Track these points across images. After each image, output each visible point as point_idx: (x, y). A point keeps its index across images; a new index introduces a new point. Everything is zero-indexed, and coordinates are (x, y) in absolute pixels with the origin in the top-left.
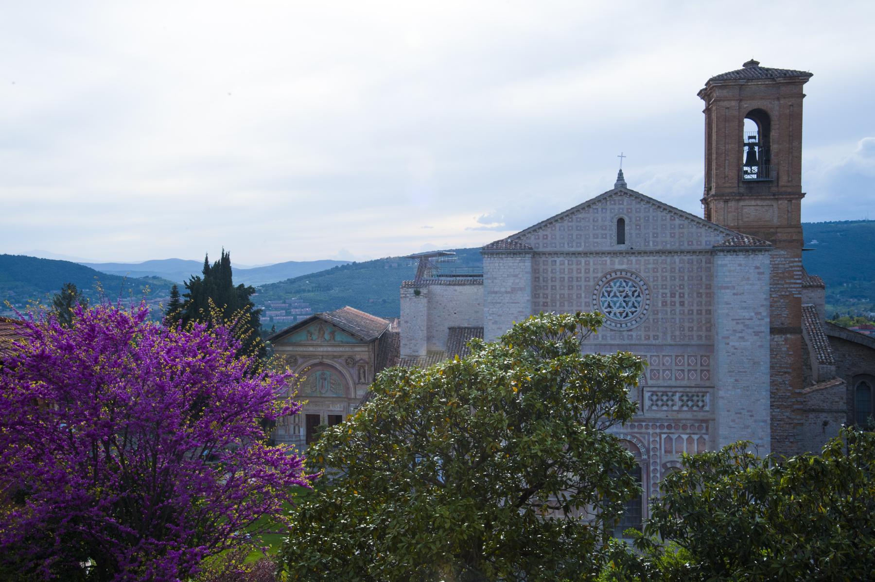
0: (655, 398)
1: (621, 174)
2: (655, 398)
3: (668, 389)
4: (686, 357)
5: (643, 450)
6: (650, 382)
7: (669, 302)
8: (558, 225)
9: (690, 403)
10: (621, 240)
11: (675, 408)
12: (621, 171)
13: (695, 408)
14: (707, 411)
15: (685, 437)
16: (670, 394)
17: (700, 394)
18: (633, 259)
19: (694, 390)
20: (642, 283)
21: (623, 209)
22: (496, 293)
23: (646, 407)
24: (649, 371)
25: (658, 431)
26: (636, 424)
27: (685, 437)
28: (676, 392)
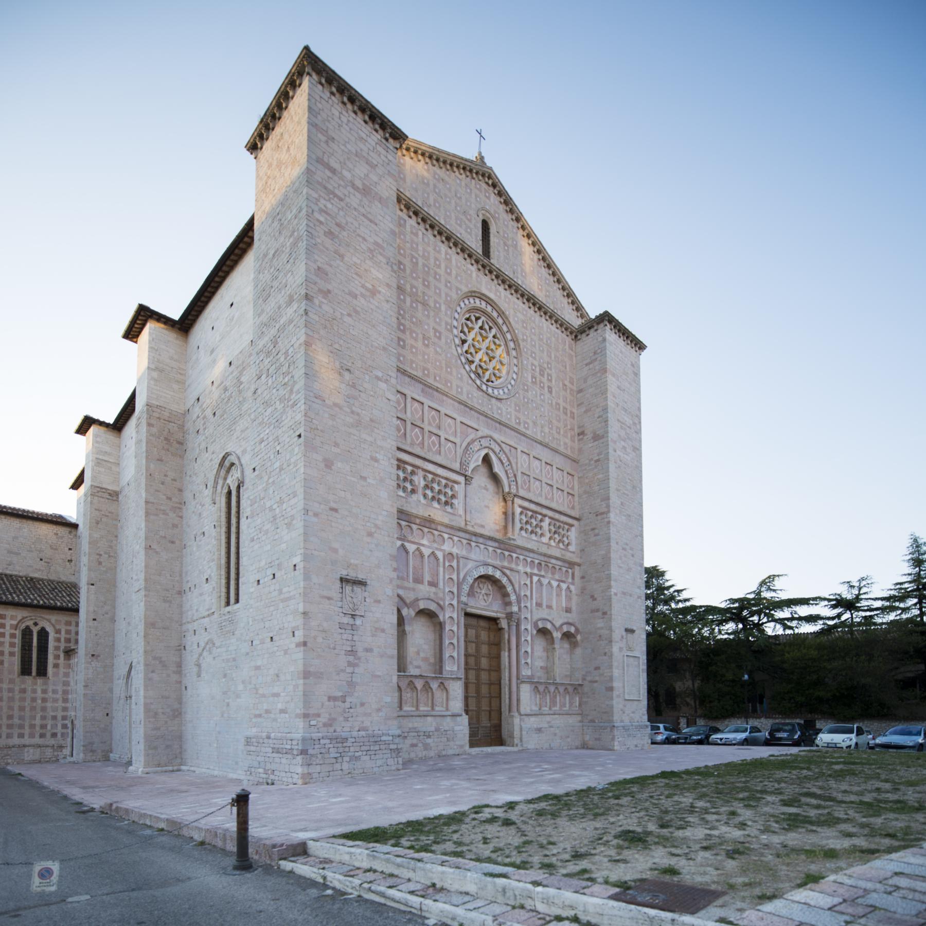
3: (538, 509)
5: (513, 598)
11: (545, 540)
14: (573, 553)
15: (555, 584)
28: (545, 516)
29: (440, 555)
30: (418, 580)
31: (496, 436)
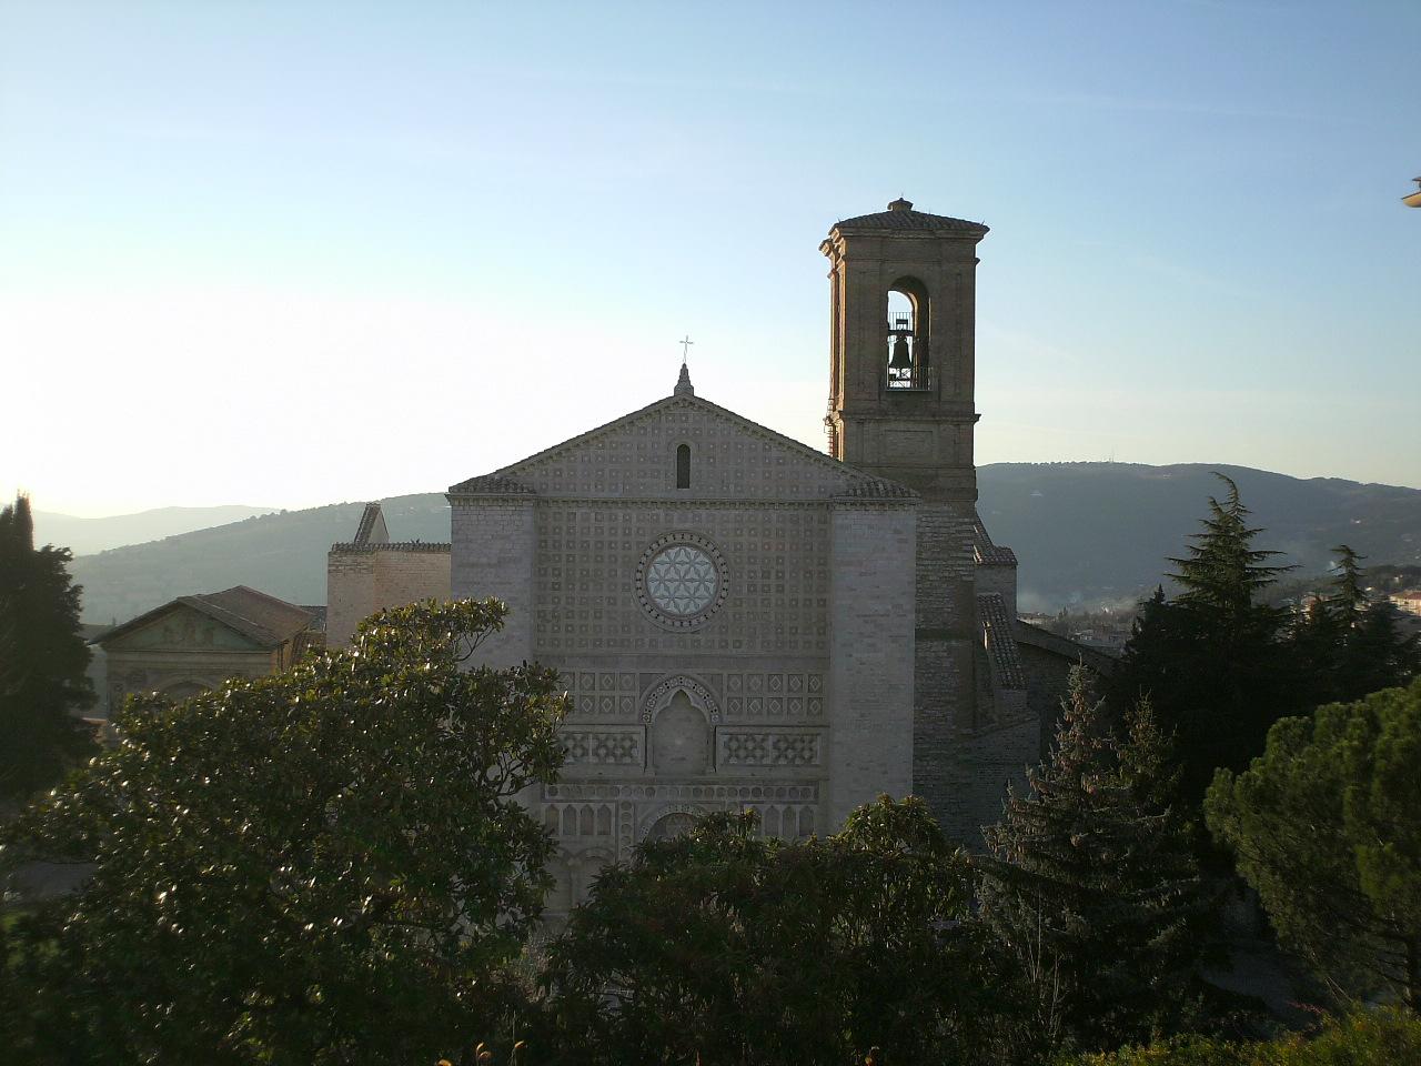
0: (734, 745)
1: (684, 371)
2: (734, 745)
3: (756, 730)
4: (785, 678)
6: (727, 719)
7: (759, 588)
8: (579, 453)
9: (790, 753)
10: (683, 481)
12: (684, 365)
13: (798, 761)
14: (817, 766)
15: (781, 808)
16: (759, 738)
17: (807, 738)
18: (703, 512)
19: (797, 731)
20: (716, 553)
21: (687, 430)
22: (473, 565)
23: (720, 760)
24: (725, 699)
25: (738, 799)
26: (703, 788)
27: (781, 808)
28: (767, 735)
29: (612, 807)
30: (586, 832)
31: (689, 671)
